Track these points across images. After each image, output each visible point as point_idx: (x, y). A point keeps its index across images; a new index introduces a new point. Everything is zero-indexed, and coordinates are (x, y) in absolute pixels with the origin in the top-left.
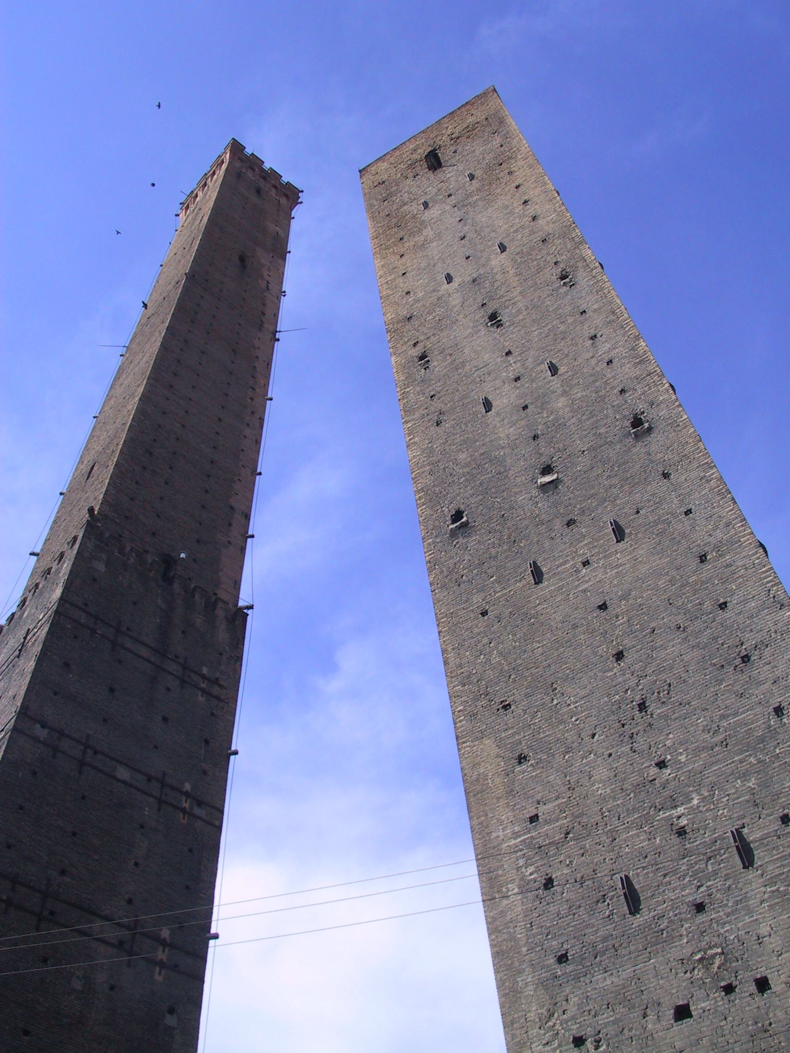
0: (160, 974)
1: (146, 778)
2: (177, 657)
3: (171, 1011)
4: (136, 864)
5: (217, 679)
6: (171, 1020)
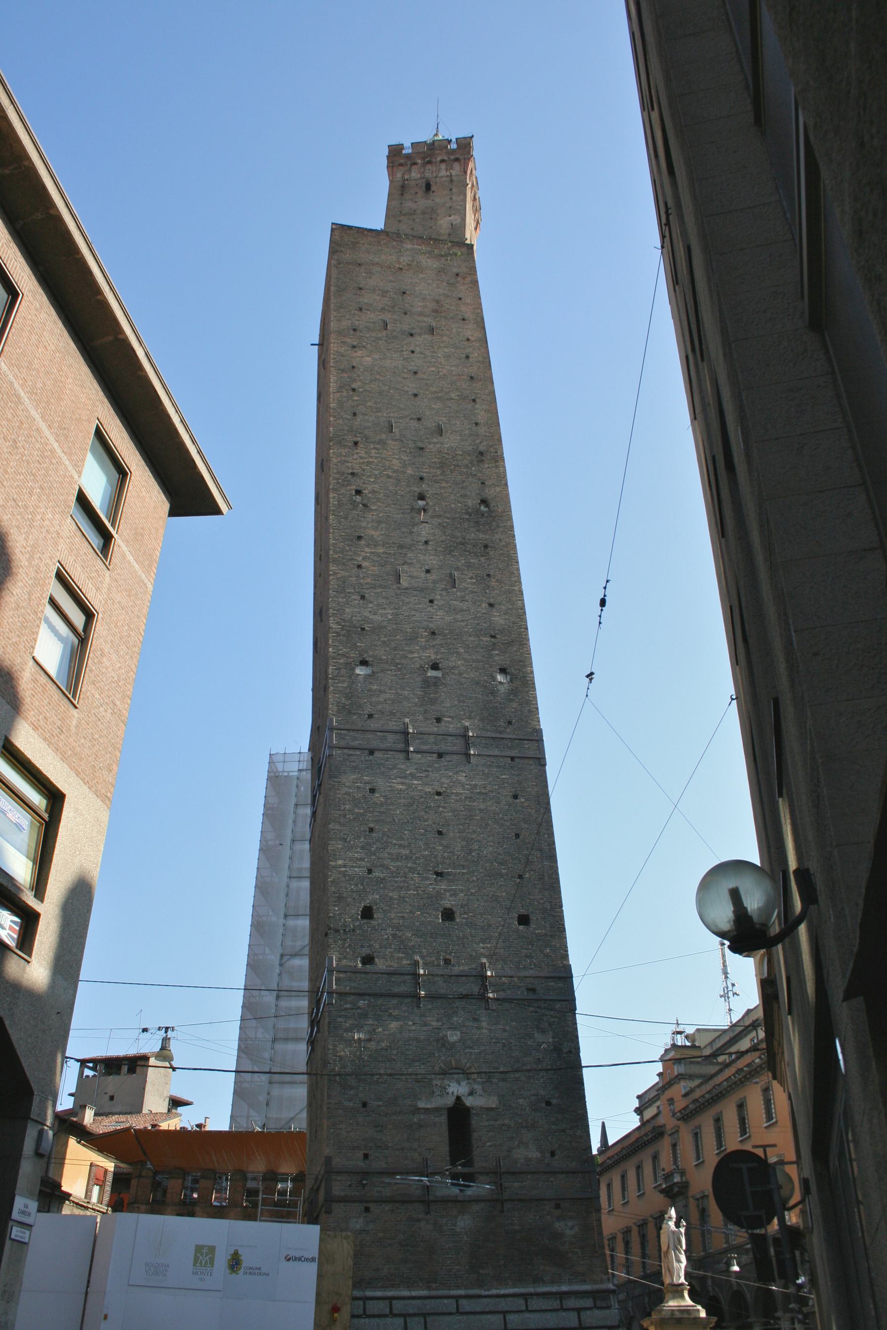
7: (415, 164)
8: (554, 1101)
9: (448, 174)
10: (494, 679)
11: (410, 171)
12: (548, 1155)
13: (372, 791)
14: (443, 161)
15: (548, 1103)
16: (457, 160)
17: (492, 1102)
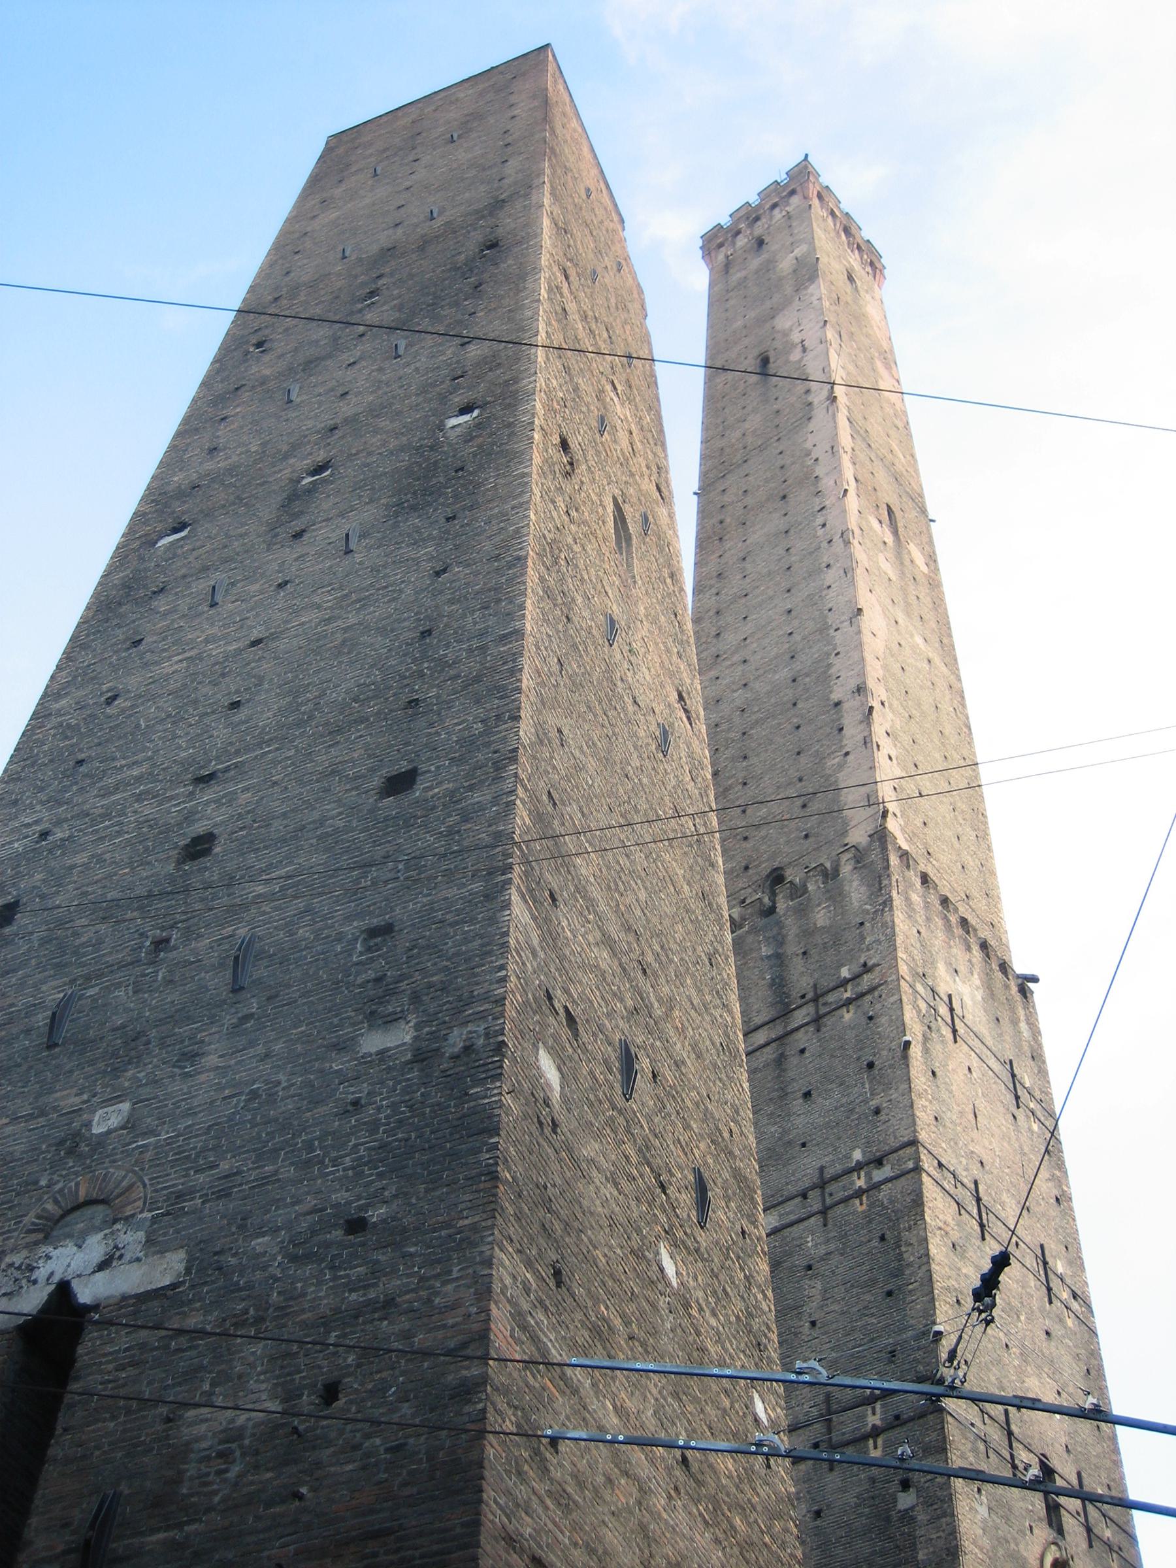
0: (875, 1447)
1: (799, 1199)
2: (803, 997)
3: (905, 1485)
4: (813, 1324)
5: (865, 965)
6: (906, 1500)
7: (738, 232)
8: (375, 1215)
9: (784, 213)
10: (441, 427)
11: (733, 243)
12: (307, 1400)
13: (110, 701)
14: (774, 206)
15: (356, 1225)
16: (793, 192)
17: (167, 1269)
